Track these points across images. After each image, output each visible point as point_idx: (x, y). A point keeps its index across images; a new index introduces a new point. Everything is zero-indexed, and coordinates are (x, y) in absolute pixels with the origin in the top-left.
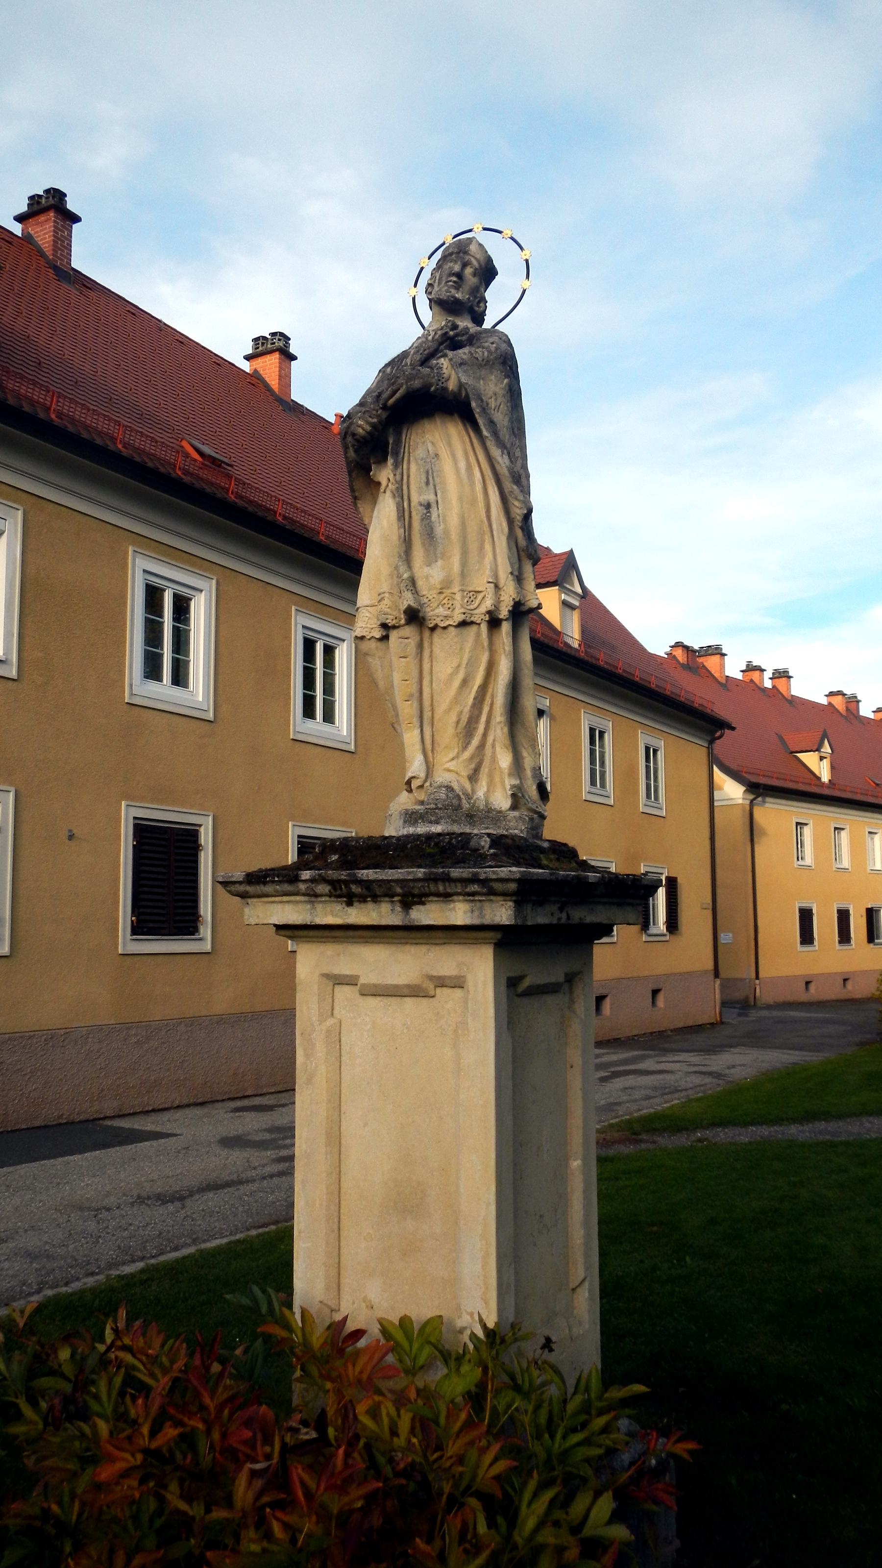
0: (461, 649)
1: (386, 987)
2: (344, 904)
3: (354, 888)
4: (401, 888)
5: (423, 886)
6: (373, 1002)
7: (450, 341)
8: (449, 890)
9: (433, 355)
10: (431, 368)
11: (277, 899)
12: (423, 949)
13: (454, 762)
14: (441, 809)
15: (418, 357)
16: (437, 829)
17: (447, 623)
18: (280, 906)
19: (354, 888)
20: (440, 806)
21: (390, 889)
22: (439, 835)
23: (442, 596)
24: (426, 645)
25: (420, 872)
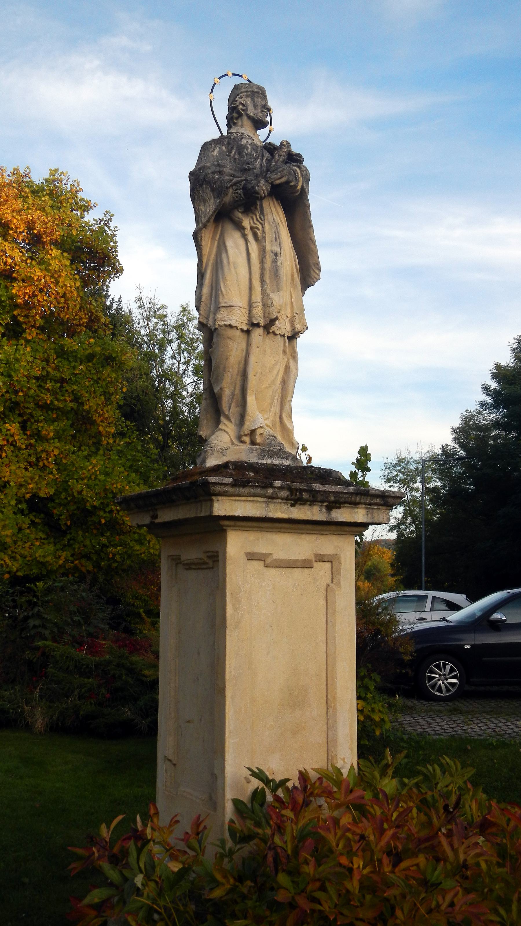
1: (289, 561)
2: (289, 506)
3: (305, 495)
4: (335, 497)
5: (348, 497)
8: (362, 501)
11: (243, 498)
12: (314, 537)
18: (242, 503)
19: (305, 495)
21: (327, 497)
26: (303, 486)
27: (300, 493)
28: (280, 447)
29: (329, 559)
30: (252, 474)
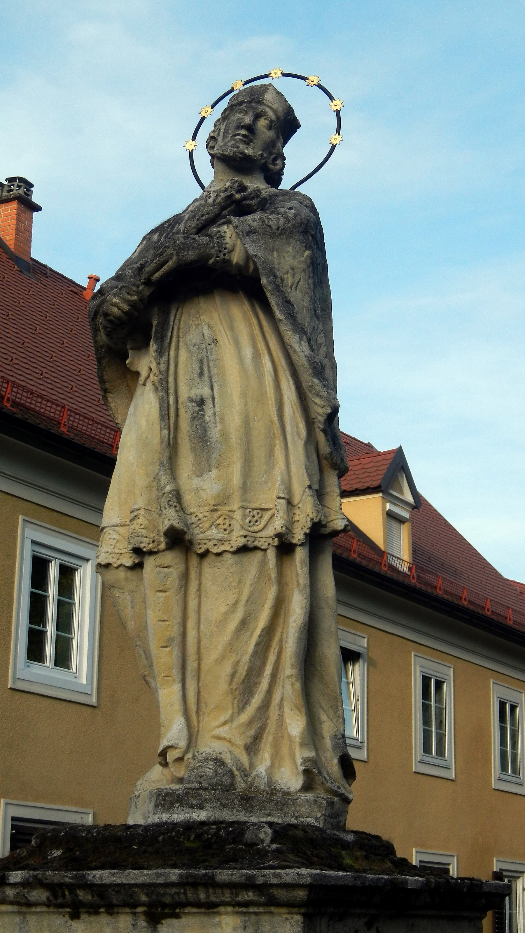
0: (240, 582)
5: (178, 894)
7: (234, 205)
9: (213, 221)
10: (210, 236)
13: (226, 728)
14: (206, 789)
15: (194, 223)
16: (201, 815)
17: (222, 548)
20: (205, 785)
21: (131, 896)
22: (203, 823)
23: (216, 515)
24: (193, 574)
25: (174, 874)
27: (70, 893)
28: (200, 783)
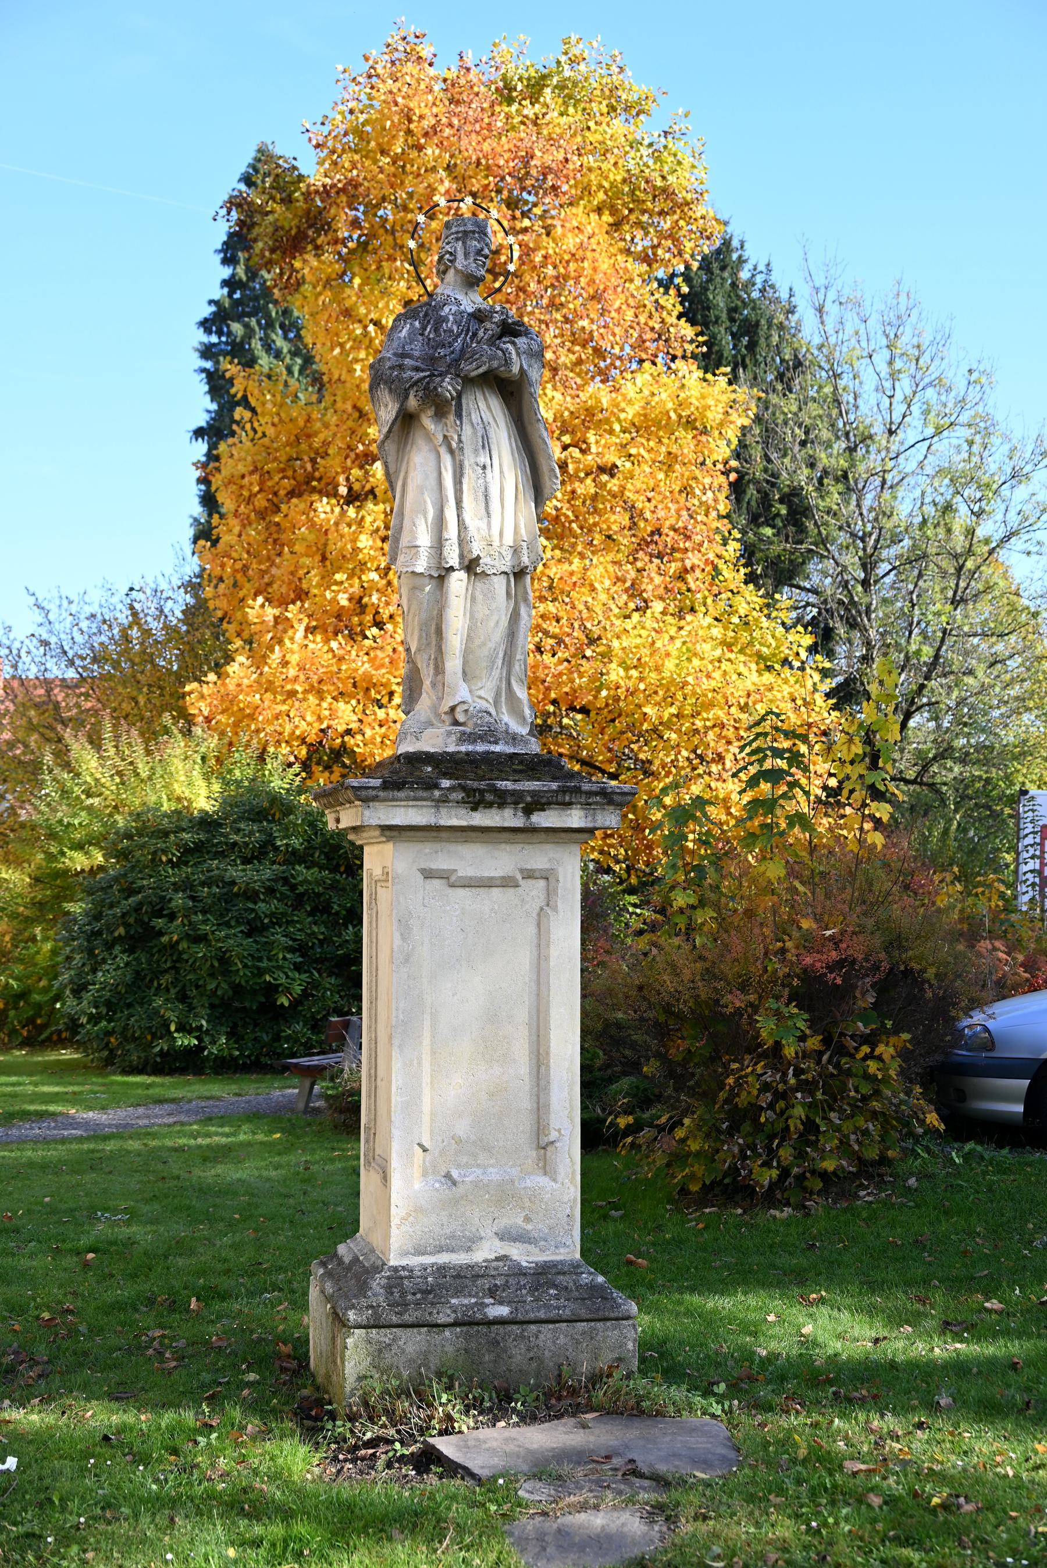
1: (481, 878)
3: (489, 797)
6: (461, 892)
16: (497, 748)
25: (554, 786)
26: (483, 785)
29: (546, 876)
30: (429, 769)
